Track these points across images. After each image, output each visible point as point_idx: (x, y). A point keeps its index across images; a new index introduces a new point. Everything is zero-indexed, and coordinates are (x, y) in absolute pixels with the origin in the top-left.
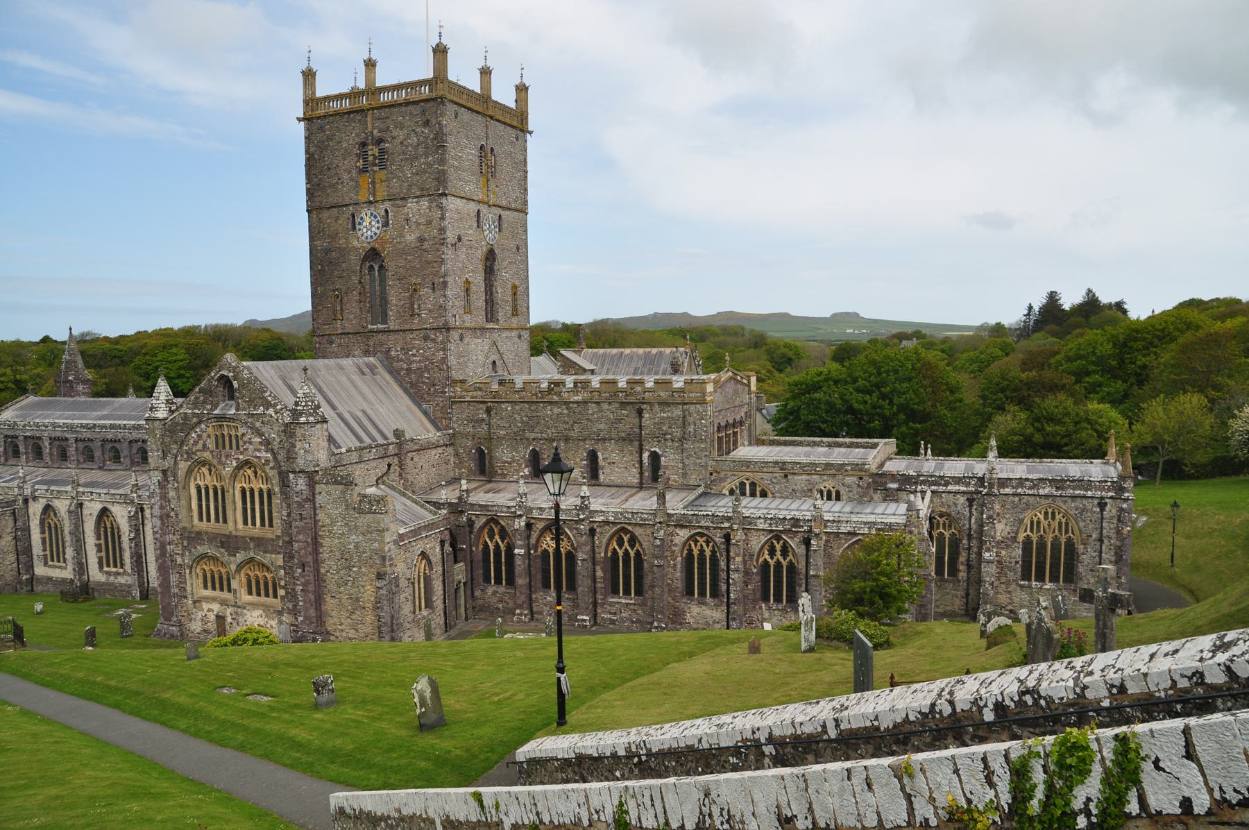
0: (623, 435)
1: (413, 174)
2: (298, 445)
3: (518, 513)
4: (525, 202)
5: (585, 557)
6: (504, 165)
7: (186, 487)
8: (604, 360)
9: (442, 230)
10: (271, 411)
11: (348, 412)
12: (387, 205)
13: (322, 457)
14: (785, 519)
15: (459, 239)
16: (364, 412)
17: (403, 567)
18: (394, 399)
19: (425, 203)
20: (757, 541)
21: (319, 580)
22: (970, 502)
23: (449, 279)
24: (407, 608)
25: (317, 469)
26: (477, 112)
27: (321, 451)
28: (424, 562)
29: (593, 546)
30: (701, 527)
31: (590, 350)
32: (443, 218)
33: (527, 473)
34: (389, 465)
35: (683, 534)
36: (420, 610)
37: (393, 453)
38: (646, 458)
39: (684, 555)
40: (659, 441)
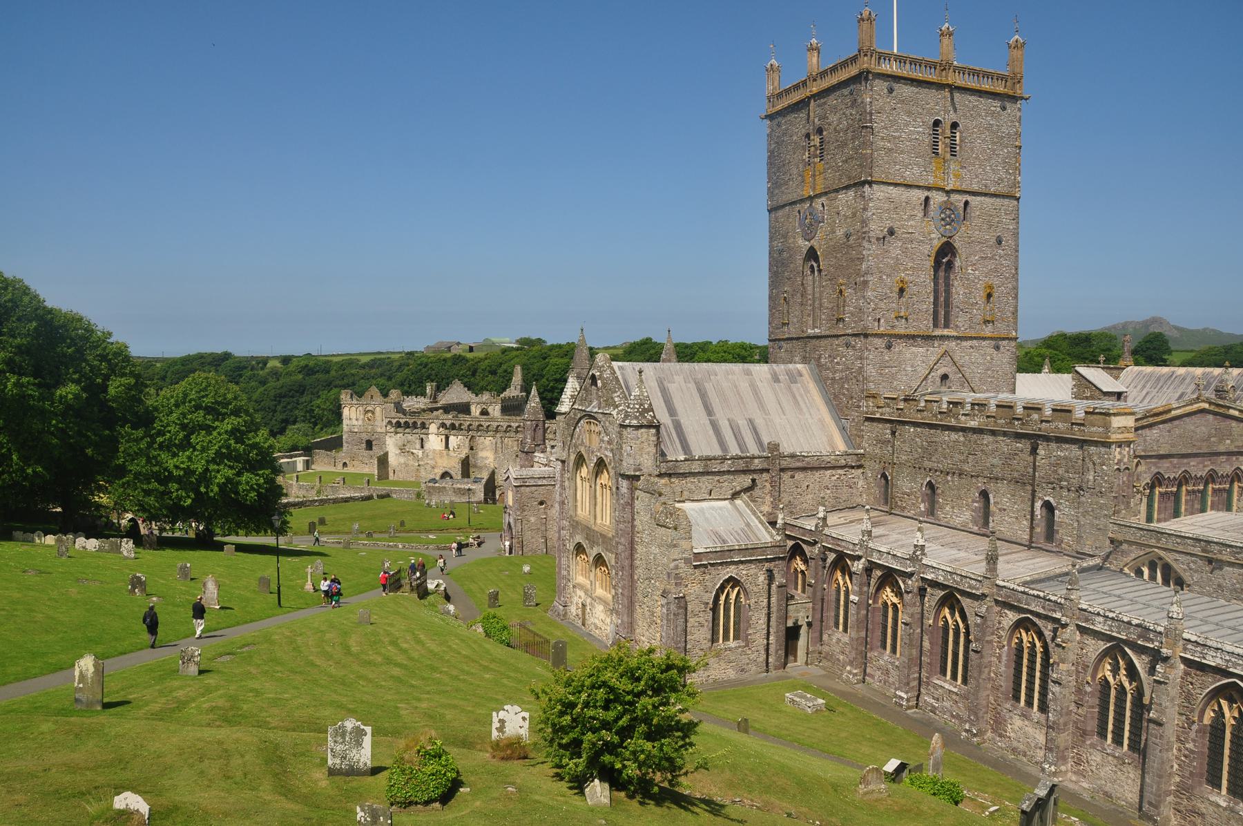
0: (1016, 475)
1: (843, 161)
2: (624, 446)
3: (857, 553)
4: (1015, 184)
5: (908, 620)
7: (573, 479)
8: (1147, 382)
9: (864, 222)
11: (729, 420)
12: (823, 199)
14: (1129, 623)
15: (891, 232)
16: (751, 422)
17: (698, 591)
18: (805, 410)
19: (851, 193)
20: (1096, 647)
24: (699, 635)
25: (637, 473)
27: (646, 456)
28: (736, 590)
29: (923, 610)
30: (1031, 612)
31: (1136, 368)
32: (865, 209)
33: (923, 509)
34: (754, 481)
35: (1012, 617)
36: (726, 638)
37: (760, 467)
38: (1039, 508)
39: (1013, 645)
40: (1054, 489)
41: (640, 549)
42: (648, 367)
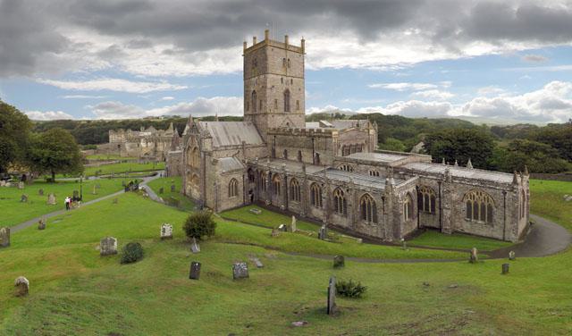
16: (238, 137)
17: (224, 182)
22: (440, 183)
23: (268, 99)
24: (226, 195)
35: (311, 182)
41: (207, 172)
42: (209, 123)
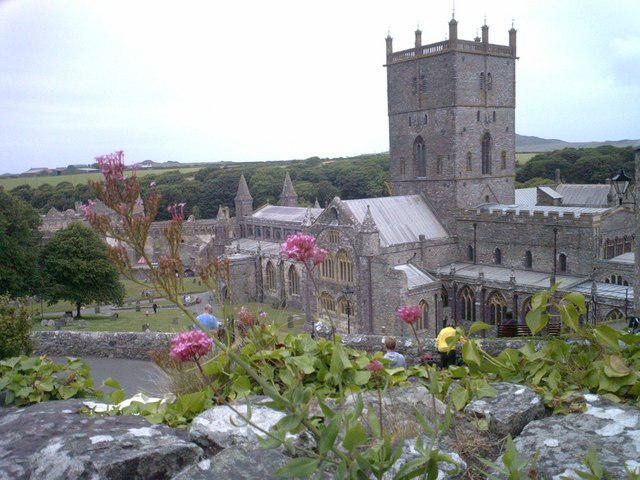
4: (514, 101)
6: (498, 82)
9: (453, 126)
10: (353, 226)
12: (426, 112)
13: (376, 252)
15: (465, 130)
21: (371, 309)
26: (479, 54)
32: (454, 119)
41: (375, 292)
